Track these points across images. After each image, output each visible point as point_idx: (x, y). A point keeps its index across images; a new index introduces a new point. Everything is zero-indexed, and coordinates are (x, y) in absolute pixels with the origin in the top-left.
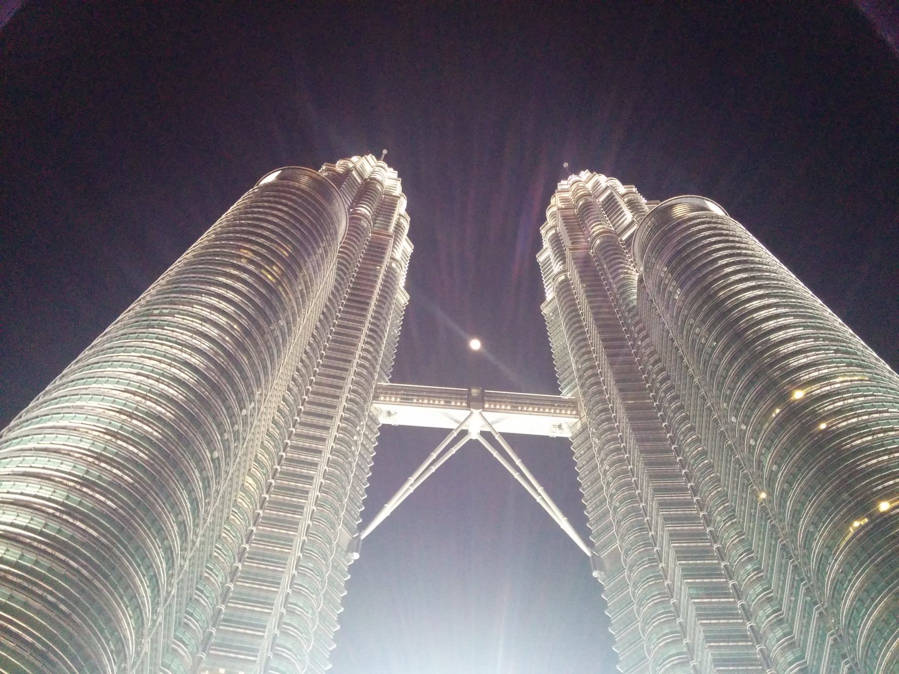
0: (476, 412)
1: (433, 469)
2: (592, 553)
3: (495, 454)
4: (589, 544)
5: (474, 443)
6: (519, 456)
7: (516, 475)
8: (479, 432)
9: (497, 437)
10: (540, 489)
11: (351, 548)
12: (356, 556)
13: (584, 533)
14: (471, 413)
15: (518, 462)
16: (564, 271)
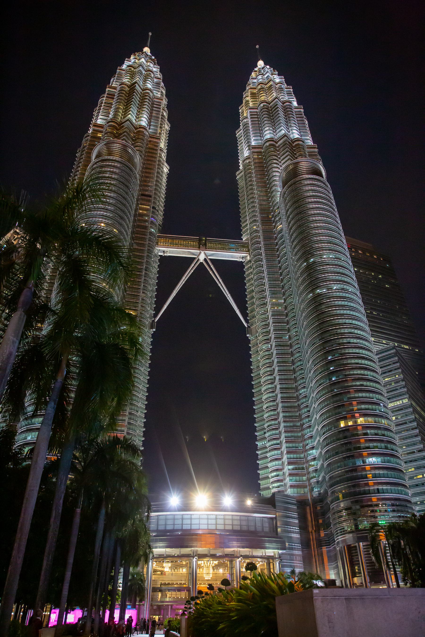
0: (203, 252)
1: (184, 283)
2: (248, 326)
3: (211, 272)
4: (247, 321)
5: (201, 263)
6: (221, 278)
7: (219, 285)
8: (204, 259)
9: (212, 266)
10: (229, 295)
11: (152, 327)
12: (154, 330)
13: (245, 315)
14: (200, 253)
15: (220, 280)
16: (248, 158)
